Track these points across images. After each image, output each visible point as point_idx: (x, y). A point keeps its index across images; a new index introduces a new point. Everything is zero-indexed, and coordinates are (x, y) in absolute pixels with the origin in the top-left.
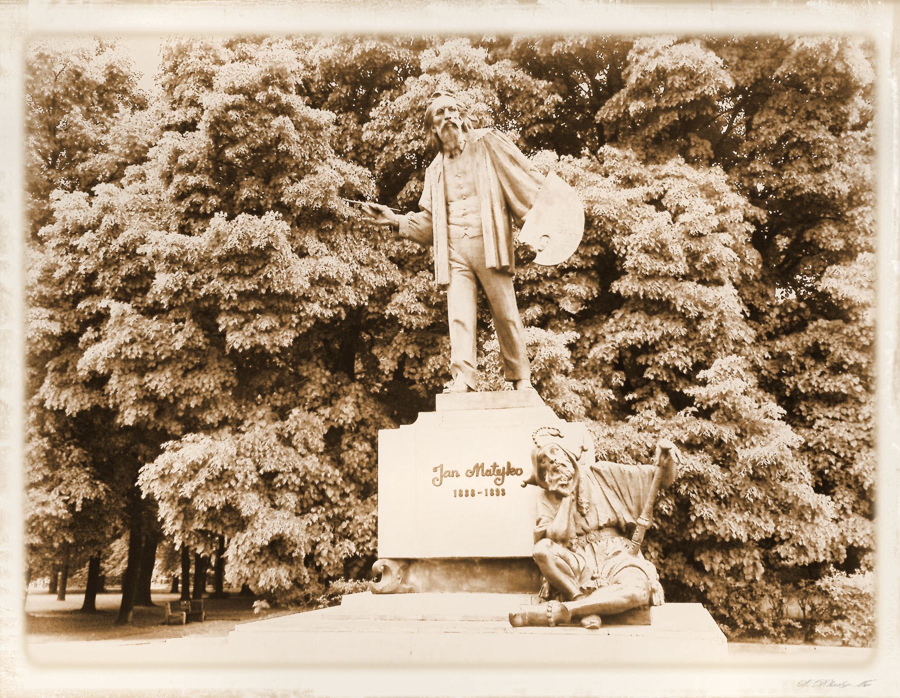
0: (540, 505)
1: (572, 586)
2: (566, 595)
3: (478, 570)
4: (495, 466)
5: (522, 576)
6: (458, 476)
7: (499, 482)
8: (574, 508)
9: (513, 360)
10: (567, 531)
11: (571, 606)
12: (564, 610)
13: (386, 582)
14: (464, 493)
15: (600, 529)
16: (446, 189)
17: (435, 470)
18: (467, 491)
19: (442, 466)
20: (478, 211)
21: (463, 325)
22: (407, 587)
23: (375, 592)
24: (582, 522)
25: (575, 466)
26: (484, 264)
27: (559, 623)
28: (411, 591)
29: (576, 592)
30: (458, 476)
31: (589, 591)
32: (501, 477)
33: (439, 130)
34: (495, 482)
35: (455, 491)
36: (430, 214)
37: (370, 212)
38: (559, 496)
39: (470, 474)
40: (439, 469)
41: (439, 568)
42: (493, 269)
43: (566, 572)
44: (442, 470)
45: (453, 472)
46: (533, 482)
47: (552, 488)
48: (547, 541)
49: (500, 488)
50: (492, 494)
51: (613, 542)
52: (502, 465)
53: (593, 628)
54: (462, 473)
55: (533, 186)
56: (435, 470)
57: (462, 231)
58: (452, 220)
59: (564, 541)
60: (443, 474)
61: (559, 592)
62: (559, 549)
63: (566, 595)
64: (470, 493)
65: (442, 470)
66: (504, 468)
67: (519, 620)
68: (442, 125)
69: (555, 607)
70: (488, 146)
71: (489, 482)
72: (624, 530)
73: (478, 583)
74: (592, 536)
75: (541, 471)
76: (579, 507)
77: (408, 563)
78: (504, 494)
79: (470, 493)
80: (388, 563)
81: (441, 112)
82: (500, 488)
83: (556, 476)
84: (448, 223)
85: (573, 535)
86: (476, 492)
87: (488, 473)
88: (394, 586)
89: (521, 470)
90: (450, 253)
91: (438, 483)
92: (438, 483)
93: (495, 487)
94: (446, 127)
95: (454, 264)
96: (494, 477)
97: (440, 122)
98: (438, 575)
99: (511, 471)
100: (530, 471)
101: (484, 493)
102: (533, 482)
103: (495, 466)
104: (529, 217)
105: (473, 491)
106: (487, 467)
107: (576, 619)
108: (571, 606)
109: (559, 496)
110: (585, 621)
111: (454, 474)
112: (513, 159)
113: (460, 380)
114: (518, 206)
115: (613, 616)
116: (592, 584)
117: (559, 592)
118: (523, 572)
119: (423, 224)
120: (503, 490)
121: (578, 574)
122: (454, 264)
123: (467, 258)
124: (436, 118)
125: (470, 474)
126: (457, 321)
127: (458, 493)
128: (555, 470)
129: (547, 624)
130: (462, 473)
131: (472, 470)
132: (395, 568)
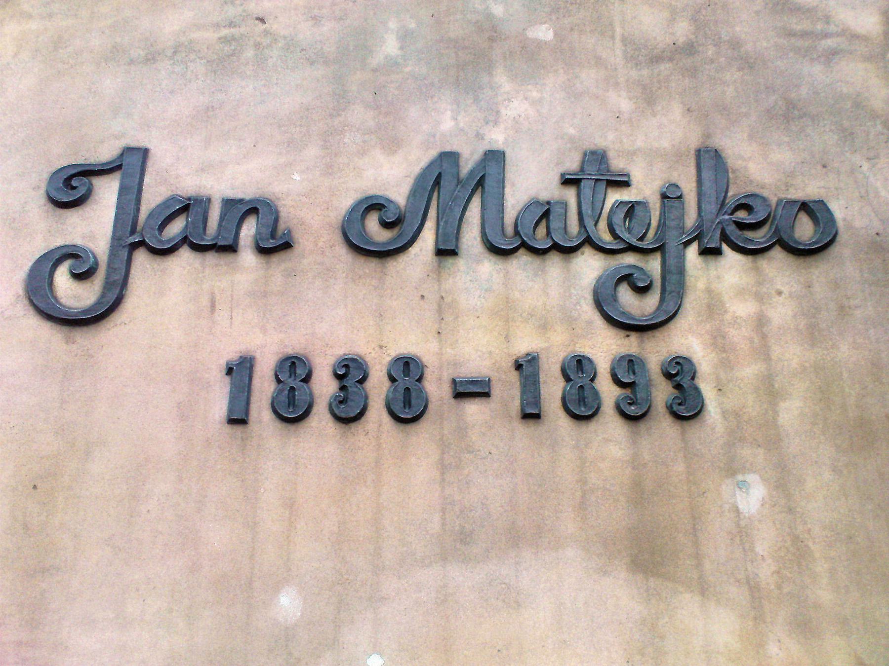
4: (594, 174)
6: (276, 245)
7: (642, 307)
14: (324, 386)
17: (70, 189)
18: (350, 372)
19: (131, 164)
30: (276, 245)
32: (654, 265)
34: (602, 302)
35: (240, 371)
39: (377, 234)
40: (107, 191)
44: (131, 195)
45: (244, 209)
49: (655, 352)
50: (581, 409)
56: (70, 189)
60: (124, 230)
64: (378, 387)
65: (131, 195)
66: (670, 197)
71: (551, 308)
78: (687, 408)
79: (378, 387)
82: (655, 352)
86: (436, 388)
87: (535, 239)
92: (76, 300)
93: (604, 347)
96: (590, 267)
101: (508, 391)
103: (594, 174)
106: (530, 180)
120: (679, 372)
125: (377, 234)
127: (264, 387)
131: (399, 194)
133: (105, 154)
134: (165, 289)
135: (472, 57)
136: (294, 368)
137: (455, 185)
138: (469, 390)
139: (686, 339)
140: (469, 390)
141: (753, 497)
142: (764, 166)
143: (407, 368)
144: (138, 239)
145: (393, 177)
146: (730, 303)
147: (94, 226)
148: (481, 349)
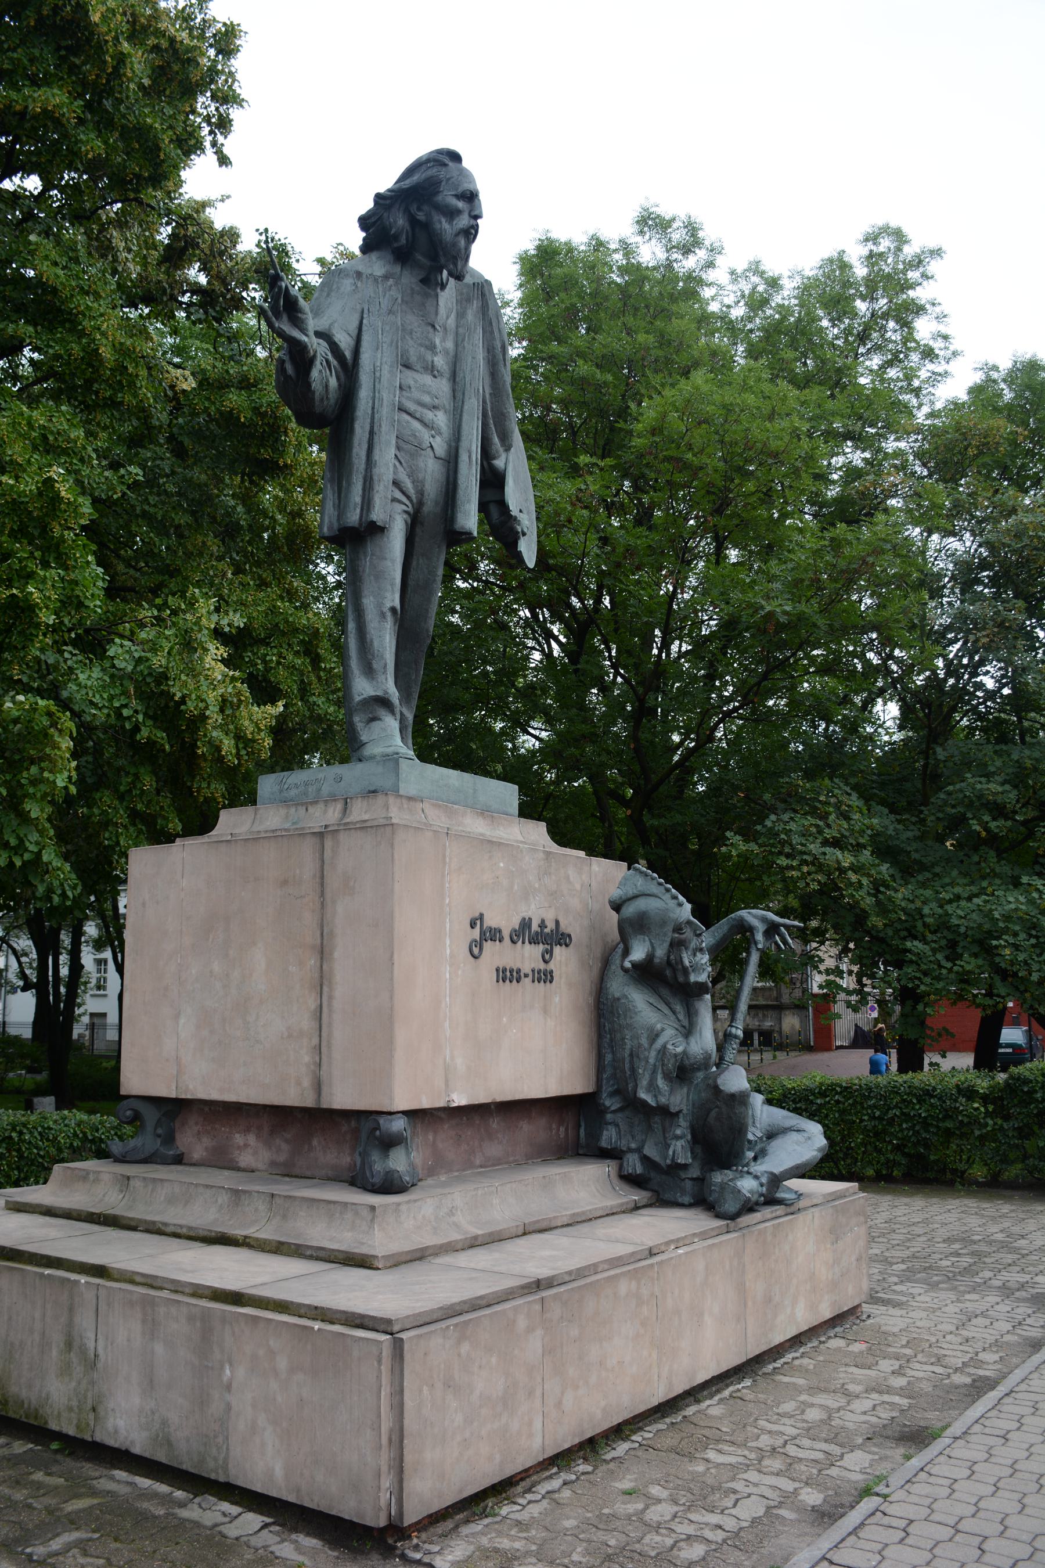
4: (542, 925)
18: (511, 971)
35: (497, 970)
41: (446, 1126)
54: (506, 934)
56: (473, 925)
73: (494, 1149)
89: (569, 936)
91: (475, 951)
96: (541, 947)
99: (561, 938)
105: (519, 971)
111: (493, 935)
118: (542, 1122)
120: (551, 972)
130: (506, 934)
133: (477, 915)
136: (504, 970)
138: (526, 976)
139: (552, 966)
140: (526, 976)
141: (557, 999)
143: (519, 971)
144: (483, 937)
145: (516, 923)
147: (476, 933)
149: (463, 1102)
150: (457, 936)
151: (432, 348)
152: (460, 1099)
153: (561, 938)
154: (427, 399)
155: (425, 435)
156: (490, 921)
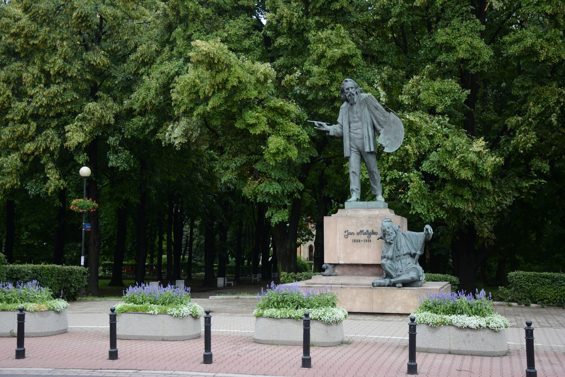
0: (383, 247)
1: (393, 273)
2: (391, 277)
3: (361, 268)
4: (368, 231)
5: (376, 270)
8: (395, 248)
9: (375, 187)
10: (392, 256)
11: (393, 280)
12: (390, 281)
13: (326, 272)
15: (404, 255)
16: (349, 118)
17: (345, 232)
20: (362, 128)
21: (355, 173)
22: (335, 274)
23: (324, 275)
24: (398, 253)
25: (396, 233)
26: (364, 149)
27: (388, 286)
28: (336, 275)
29: (394, 275)
31: (399, 276)
33: (347, 96)
36: (342, 126)
37: (317, 125)
38: (390, 244)
39: (358, 234)
42: (368, 153)
43: (392, 270)
46: (381, 238)
47: (388, 241)
48: (385, 259)
51: (409, 260)
52: (370, 231)
53: (399, 287)
55: (384, 119)
56: (345, 232)
57: (356, 136)
58: (351, 131)
59: (392, 259)
60: (348, 234)
61: (389, 276)
62: (389, 262)
63: (391, 277)
67: (375, 285)
68: (349, 93)
69: (387, 281)
70: (367, 102)
71: (365, 237)
72: (413, 256)
73: (361, 273)
74: (401, 257)
75: (385, 235)
76: (397, 247)
77: (335, 265)
80: (328, 265)
81: (348, 89)
83: (389, 237)
84: (350, 131)
85: (395, 257)
87: (365, 234)
88: (330, 274)
90: (350, 144)
91: (346, 237)
92: (346, 237)
94: (350, 95)
95: (352, 149)
97: (347, 93)
98: (346, 269)
99: (374, 233)
100: (380, 234)
102: (381, 238)
103: (368, 231)
104: (382, 132)
106: (365, 231)
107: (394, 285)
108: (393, 280)
109: (390, 244)
110: (397, 285)
111: (352, 234)
112: (376, 108)
113: (355, 196)
114: (378, 127)
115: (406, 284)
116: (400, 273)
117: (389, 276)
119: (339, 130)
121: (396, 270)
122: (352, 149)
123: (357, 147)
124: (346, 91)
125: (358, 234)
126: (353, 172)
128: (389, 235)
129: (385, 286)
132: (330, 267)
134: (349, 236)
135: (362, 225)
137: (361, 231)
142: (375, 231)
146: (373, 236)
147: (346, 234)
148: (362, 239)
149: (343, 263)
150: (340, 234)
151: (354, 118)
152: (341, 262)
153: (374, 233)
154: (355, 128)
155: (356, 136)
156: (350, 231)
